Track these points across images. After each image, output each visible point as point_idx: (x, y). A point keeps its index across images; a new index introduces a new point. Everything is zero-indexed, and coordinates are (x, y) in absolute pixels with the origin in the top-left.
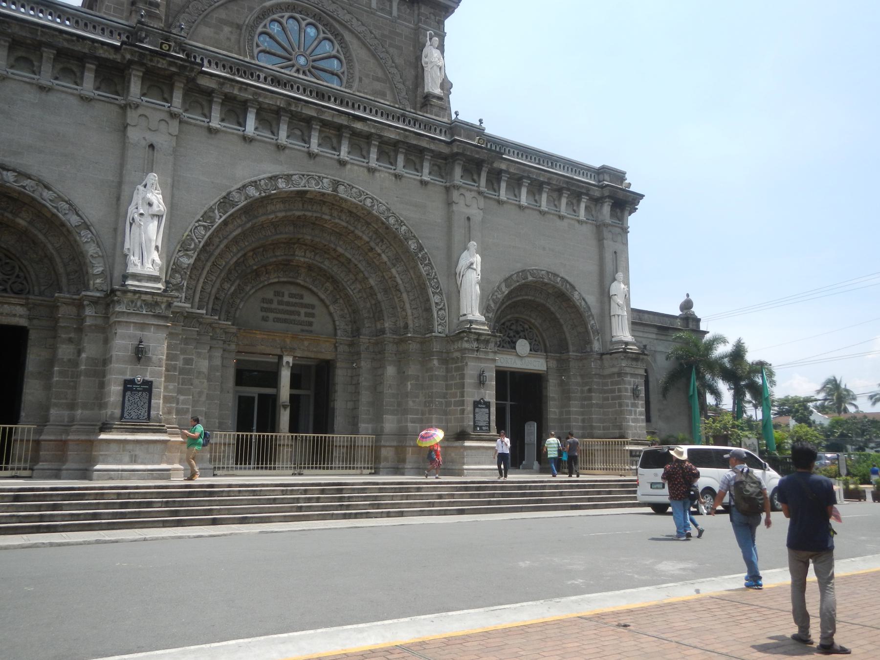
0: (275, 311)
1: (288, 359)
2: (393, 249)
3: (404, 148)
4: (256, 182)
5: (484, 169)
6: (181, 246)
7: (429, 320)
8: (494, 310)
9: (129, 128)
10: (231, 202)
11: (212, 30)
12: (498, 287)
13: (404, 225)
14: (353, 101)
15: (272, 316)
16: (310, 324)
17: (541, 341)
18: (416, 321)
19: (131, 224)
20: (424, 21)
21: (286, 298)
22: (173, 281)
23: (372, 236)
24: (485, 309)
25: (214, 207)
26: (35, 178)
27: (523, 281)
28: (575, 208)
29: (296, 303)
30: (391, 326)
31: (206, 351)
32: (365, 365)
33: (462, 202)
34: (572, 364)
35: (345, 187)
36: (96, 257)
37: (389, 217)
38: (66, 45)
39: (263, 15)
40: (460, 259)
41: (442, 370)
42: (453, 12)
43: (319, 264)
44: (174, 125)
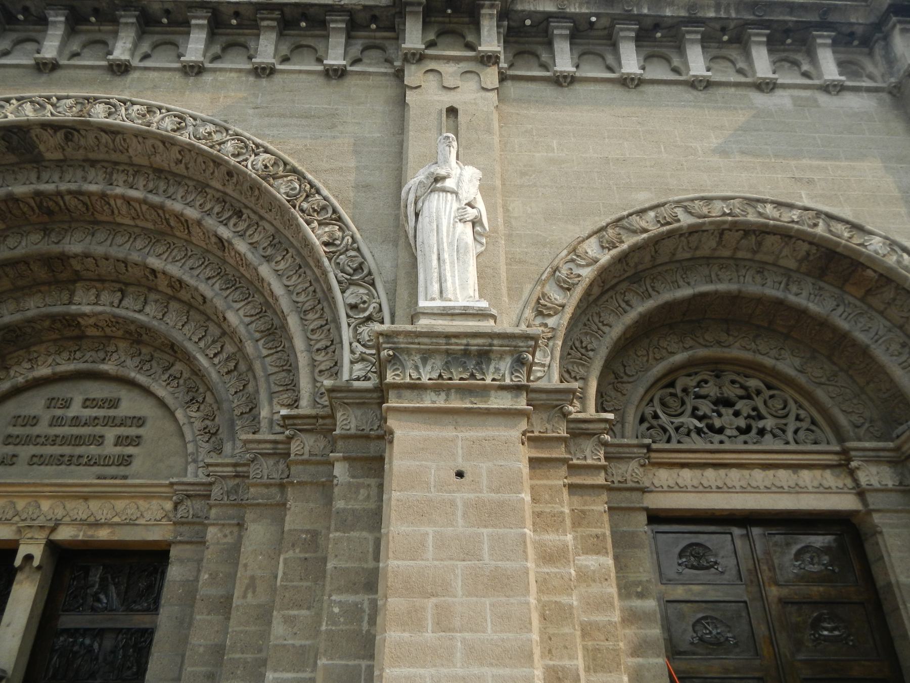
2: (267, 226)
3: (272, 19)
8: (563, 306)
13: (266, 151)
15: (26, 452)
16: (126, 461)
21: (75, 410)
23: (212, 208)
27: (665, 228)
28: (805, 67)
29: (96, 418)
41: (363, 492)
43: (131, 314)
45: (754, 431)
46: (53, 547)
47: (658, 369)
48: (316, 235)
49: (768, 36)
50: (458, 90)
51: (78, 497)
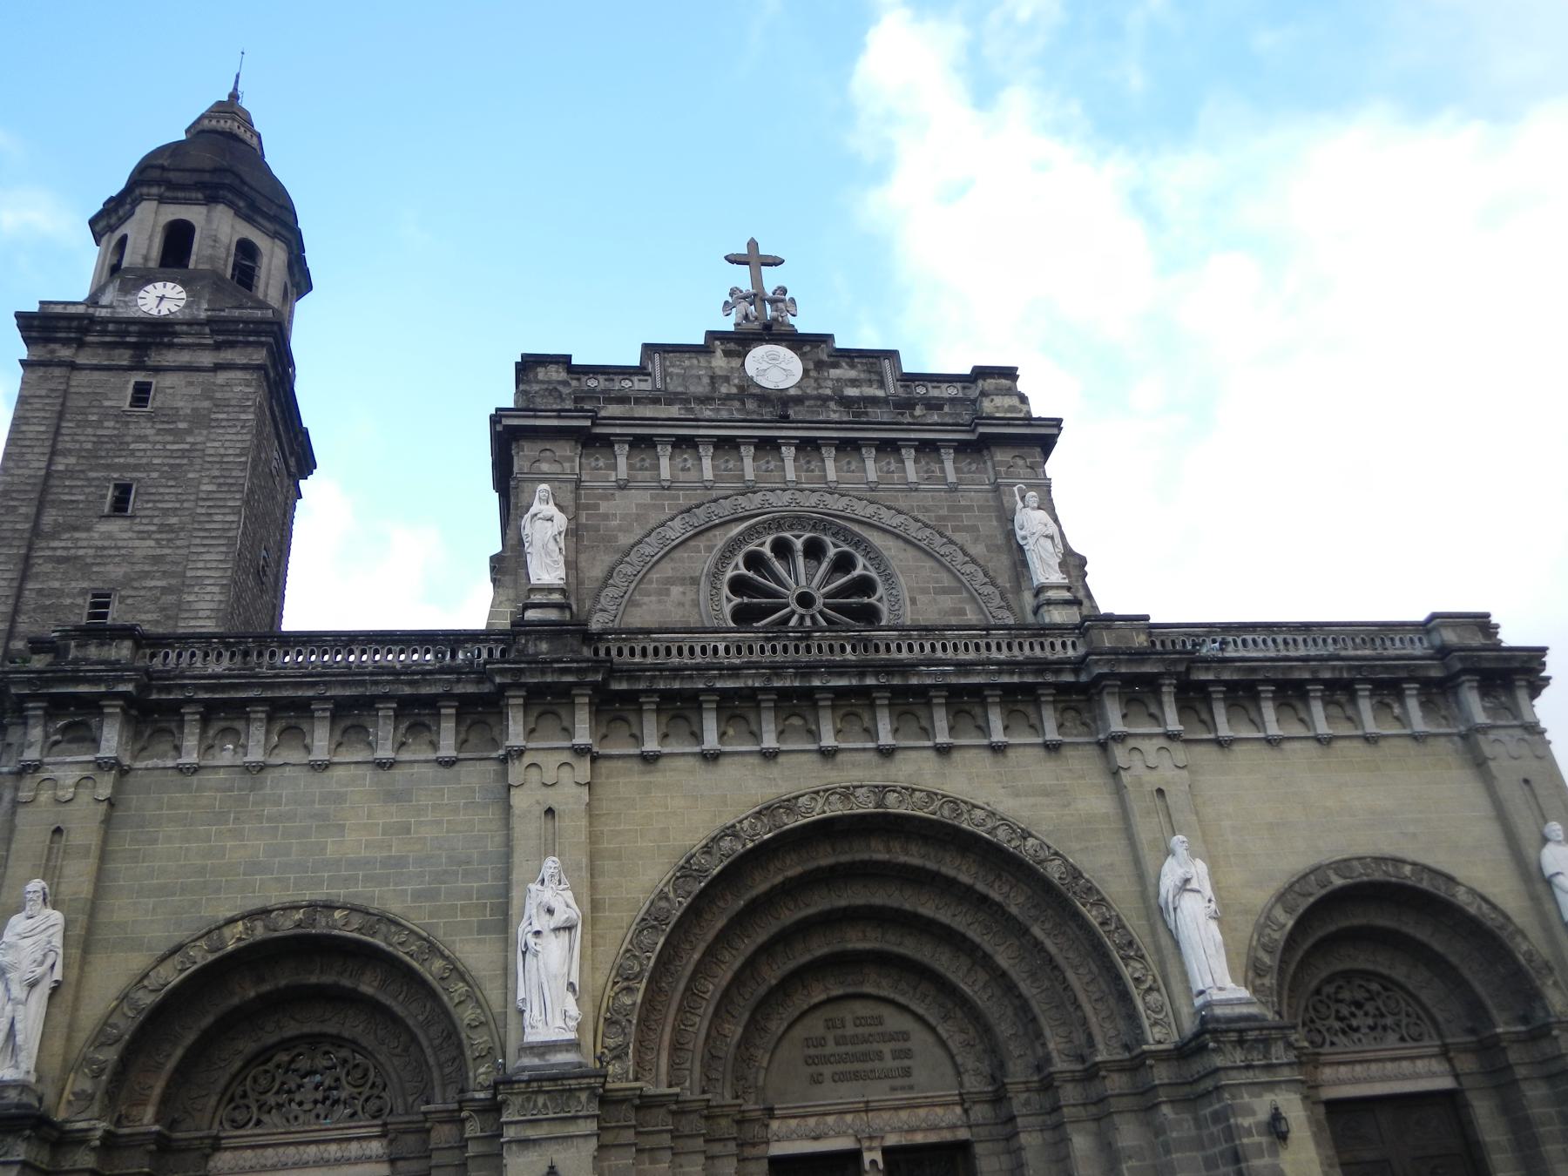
0: (832, 1059)
1: (872, 1156)
3: (996, 696)
4: (734, 826)
5: (1164, 689)
6: (617, 975)
7: (1132, 1017)
8: (1270, 967)
9: (513, 792)
10: (695, 873)
11: (653, 598)
12: (1268, 918)
14: (885, 641)
15: (827, 1070)
16: (907, 1072)
17: (1422, 1014)
18: (1107, 1025)
19: (524, 953)
20: (1006, 473)
21: (850, 1030)
22: (610, 1042)
23: (976, 873)
24: (1252, 971)
25: (666, 890)
26: (376, 911)
27: (1323, 892)
29: (870, 1035)
30: (1061, 1046)
31: (700, 1168)
32: (1030, 1140)
33: (1137, 762)
34: (1513, 1056)
35: (899, 793)
36: (476, 1027)
37: (995, 828)
38: (407, 690)
39: (730, 551)
40: (1162, 877)
42: (1054, 443)
44: (583, 768)
45: (1380, 1028)
46: (887, 1152)
47: (1314, 984)
48: (1092, 916)
49: (1370, 690)
50: (1159, 769)
51: (890, 1109)
